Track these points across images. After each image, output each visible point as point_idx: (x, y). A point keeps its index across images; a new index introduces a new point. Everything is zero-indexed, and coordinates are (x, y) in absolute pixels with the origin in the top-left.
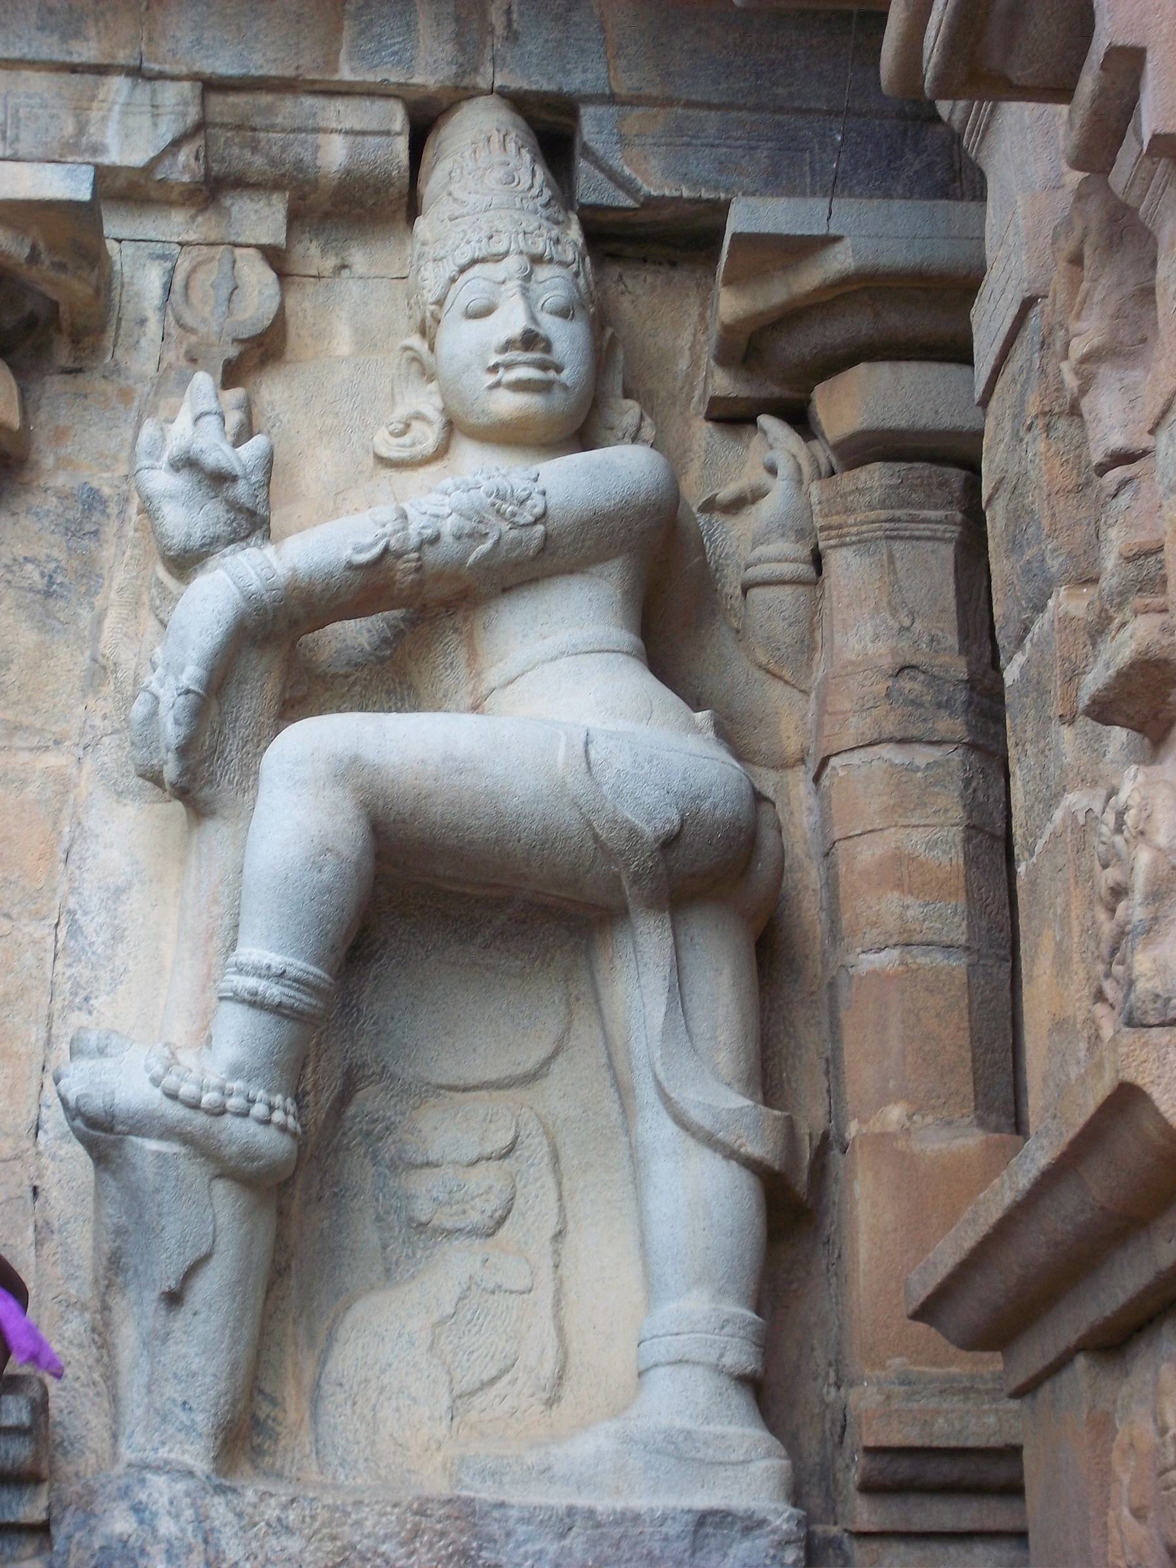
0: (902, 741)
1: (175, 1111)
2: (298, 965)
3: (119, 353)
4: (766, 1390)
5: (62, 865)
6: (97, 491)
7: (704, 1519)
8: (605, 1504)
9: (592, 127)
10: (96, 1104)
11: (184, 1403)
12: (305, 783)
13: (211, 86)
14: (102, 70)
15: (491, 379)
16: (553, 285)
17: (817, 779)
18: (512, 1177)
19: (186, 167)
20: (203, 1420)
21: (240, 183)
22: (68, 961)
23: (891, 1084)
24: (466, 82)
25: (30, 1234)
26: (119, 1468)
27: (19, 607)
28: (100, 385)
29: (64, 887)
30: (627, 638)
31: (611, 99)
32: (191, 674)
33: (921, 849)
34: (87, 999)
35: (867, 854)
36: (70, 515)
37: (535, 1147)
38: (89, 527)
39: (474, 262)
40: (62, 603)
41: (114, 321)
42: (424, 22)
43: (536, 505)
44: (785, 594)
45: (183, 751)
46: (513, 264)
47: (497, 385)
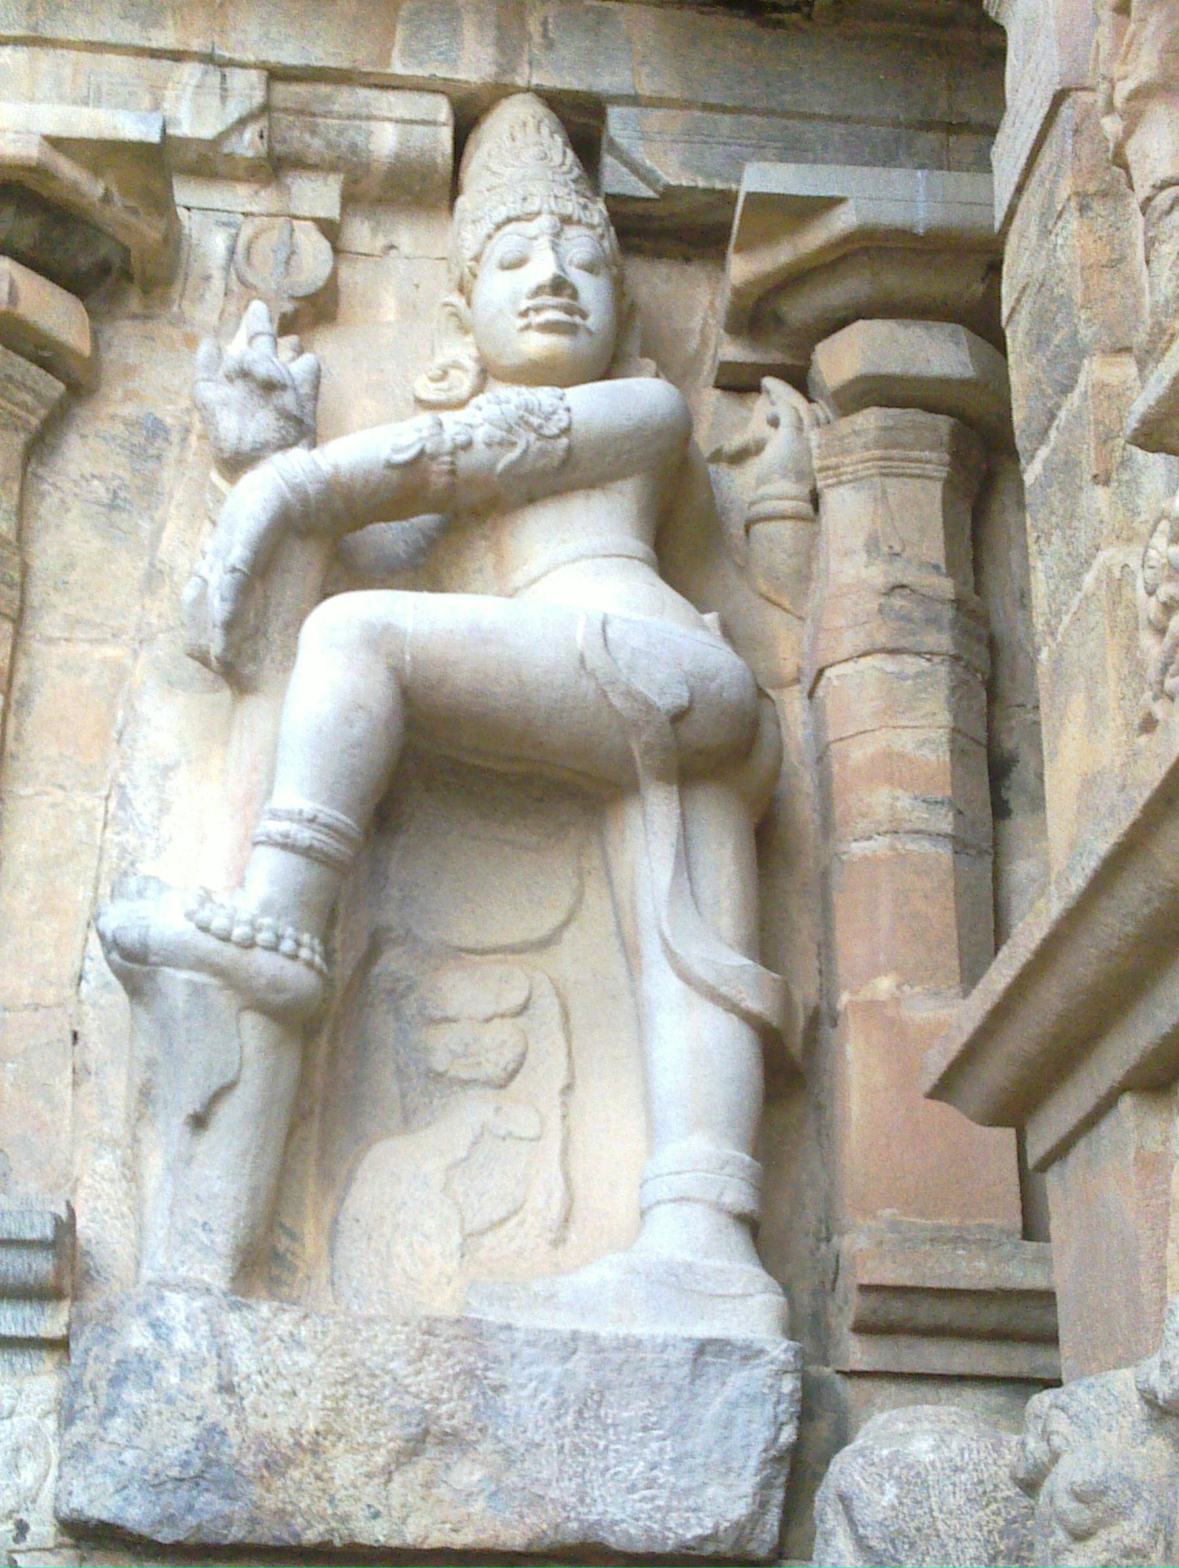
0: (893, 652)
1: (209, 944)
2: (330, 814)
3: (186, 304)
4: (764, 1231)
5: (114, 745)
6: (161, 421)
7: (702, 1348)
8: (607, 1330)
9: (619, 125)
10: (131, 937)
11: (205, 1224)
12: (340, 651)
13: (276, 75)
14: (177, 56)
15: (522, 322)
16: (581, 245)
17: (811, 695)
18: (524, 1034)
19: (252, 143)
20: (223, 1241)
21: (299, 163)
22: (117, 829)
23: (882, 957)
24: (506, 80)
25: (68, 1073)
26: (140, 1288)
27: (85, 516)
28: (167, 330)
30: (640, 547)
31: (634, 100)
32: (238, 552)
33: (910, 747)
34: (132, 864)
35: (859, 753)
36: (135, 440)
37: (547, 1006)
38: (152, 451)
39: (509, 220)
40: (125, 516)
41: (181, 277)
42: (469, 31)
43: (561, 420)
44: (785, 530)
45: (229, 626)
46: (544, 222)
47: (527, 327)
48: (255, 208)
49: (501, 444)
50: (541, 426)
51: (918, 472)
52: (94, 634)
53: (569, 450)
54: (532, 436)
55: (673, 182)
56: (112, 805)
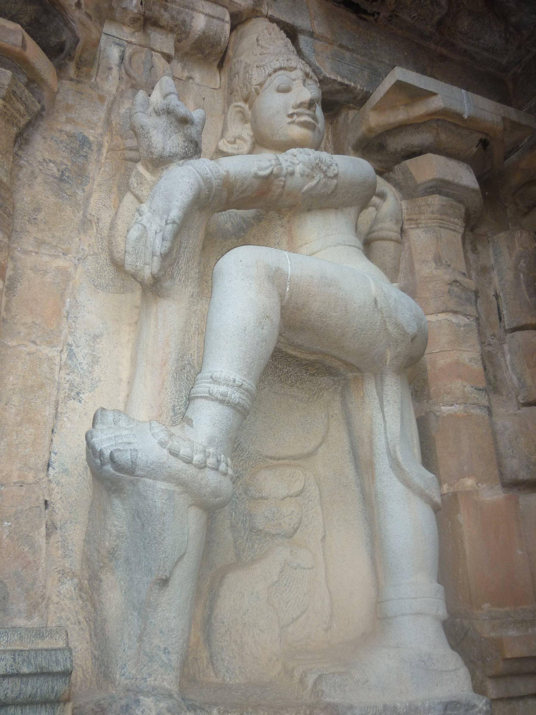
0: (456, 312)
3: (98, 79)
5: (65, 319)
6: (87, 138)
19: (136, 6)
21: (156, 24)
22: (68, 371)
27: (46, 183)
29: (66, 331)
31: (311, 34)
34: (78, 394)
36: (73, 145)
39: (281, 69)
40: (68, 186)
41: (96, 64)
47: (293, 122)
48: (133, 40)
49: (308, 176)
50: (326, 171)
51: (453, 228)
52: (52, 252)
53: (336, 186)
54: (322, 175)
55: (328, 76)
56: (64, 356)
